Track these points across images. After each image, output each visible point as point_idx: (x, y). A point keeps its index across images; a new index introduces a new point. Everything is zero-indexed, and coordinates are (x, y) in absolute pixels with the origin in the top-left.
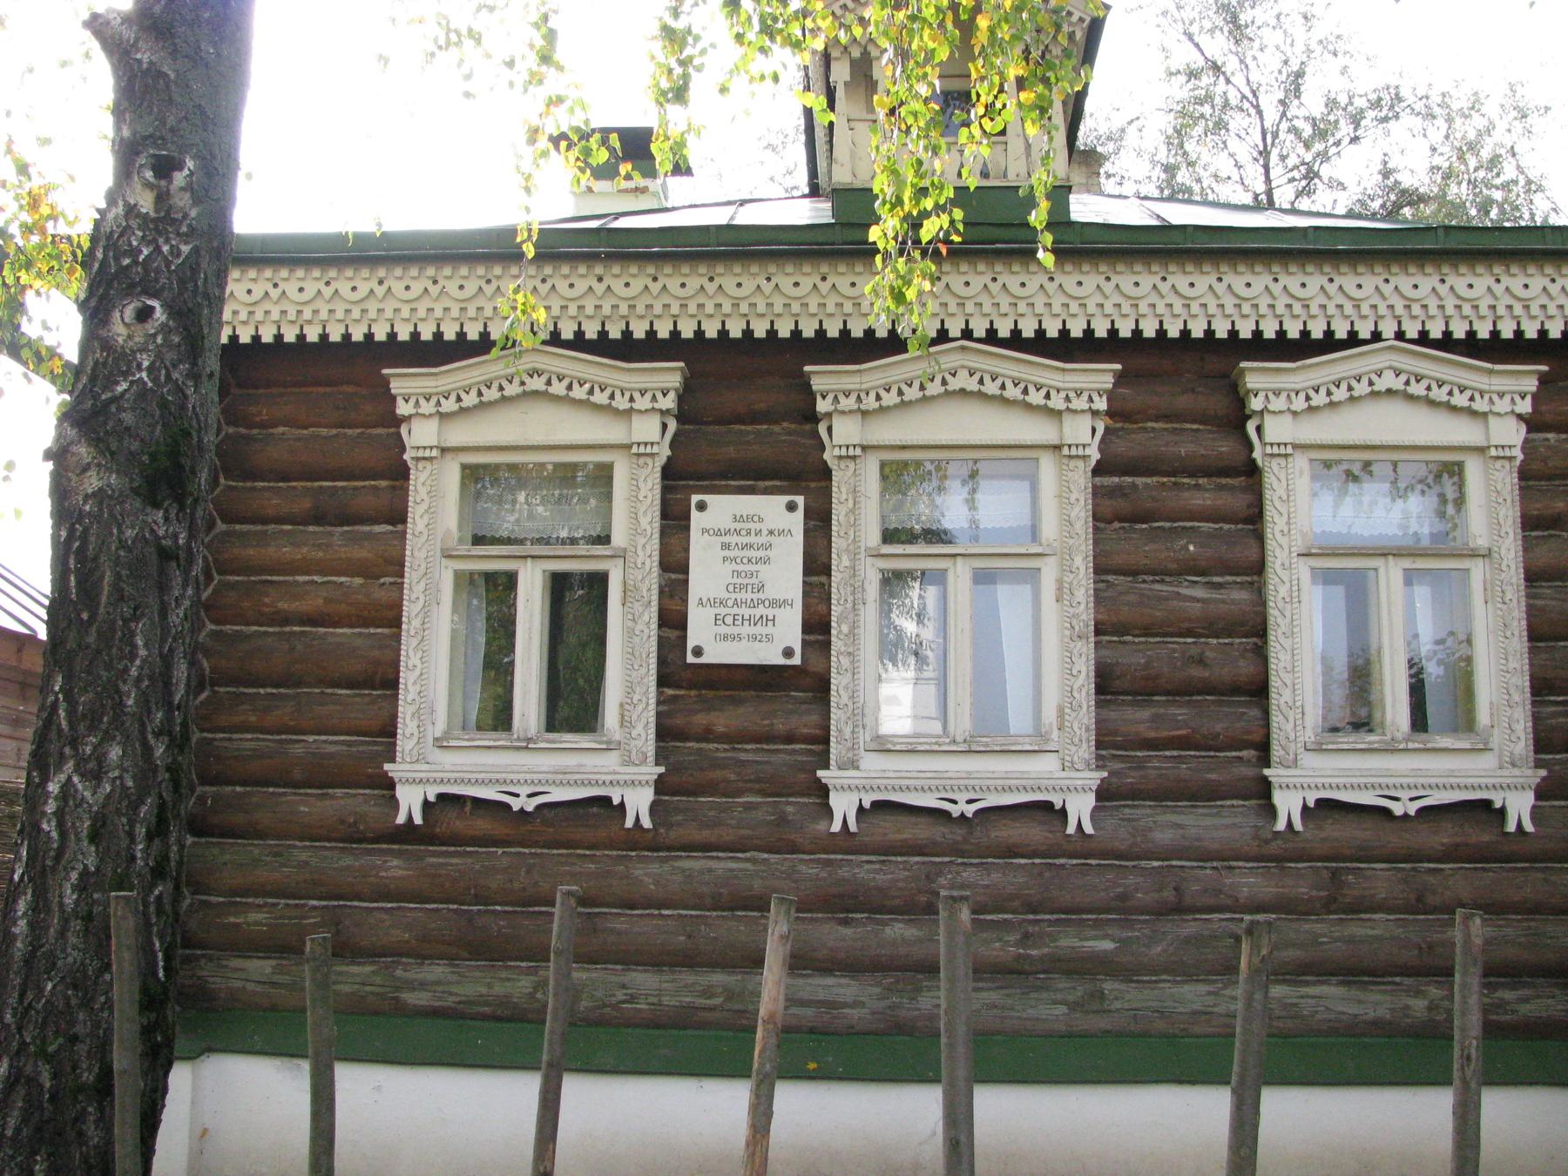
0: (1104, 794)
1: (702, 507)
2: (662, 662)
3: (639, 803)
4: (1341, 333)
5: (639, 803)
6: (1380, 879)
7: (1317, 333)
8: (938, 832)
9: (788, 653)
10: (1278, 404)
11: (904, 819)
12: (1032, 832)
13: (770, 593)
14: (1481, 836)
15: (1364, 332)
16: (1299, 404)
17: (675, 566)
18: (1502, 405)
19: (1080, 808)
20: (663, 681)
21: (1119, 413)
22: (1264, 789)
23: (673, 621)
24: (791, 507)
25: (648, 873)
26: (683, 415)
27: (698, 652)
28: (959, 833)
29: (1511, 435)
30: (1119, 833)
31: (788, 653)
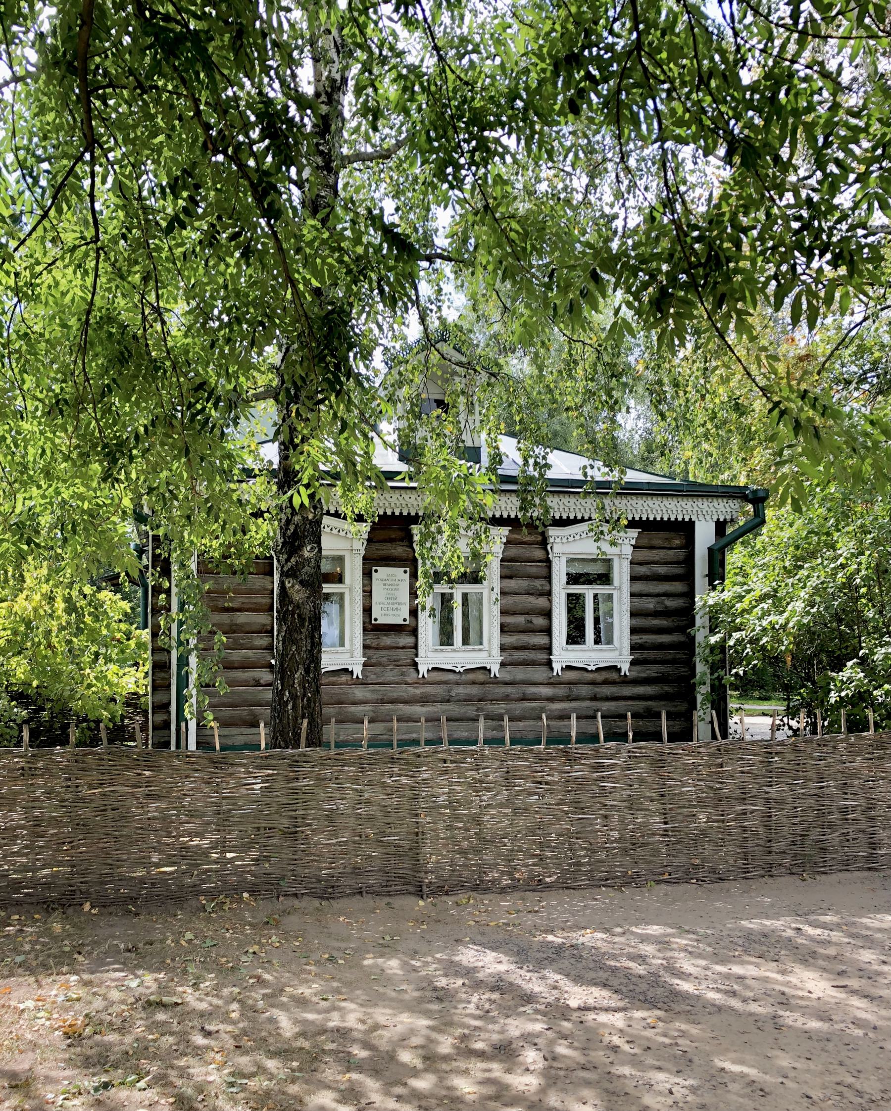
0: (503, 664)
1: (376, 571)
2: (364, 623)
3: (358, 670)
4: (579, 517)
5: (358, 670)
6: (584, 690)
7: (572, 517)
8: (451, 676)
9: (405, 620)
10: (558, 540)
11: (440, 673)
12: (480, 677)
13: (398, 601)
14: (614, 676)
15: (586, 518)
16: (565, 540)
17: (368, 593)
18: (626, 541)
19: (495, 669)
20: (365, 629)
21: (508, 543)
22: (549, 664)
23: (367, 610)
24: (405, 572)
25: (359, 693)
26: (370, 540)
27: (376, 620)
28: (458, 677)
29: (628, 550)
30: (507, 677)
31: (405, 620)
